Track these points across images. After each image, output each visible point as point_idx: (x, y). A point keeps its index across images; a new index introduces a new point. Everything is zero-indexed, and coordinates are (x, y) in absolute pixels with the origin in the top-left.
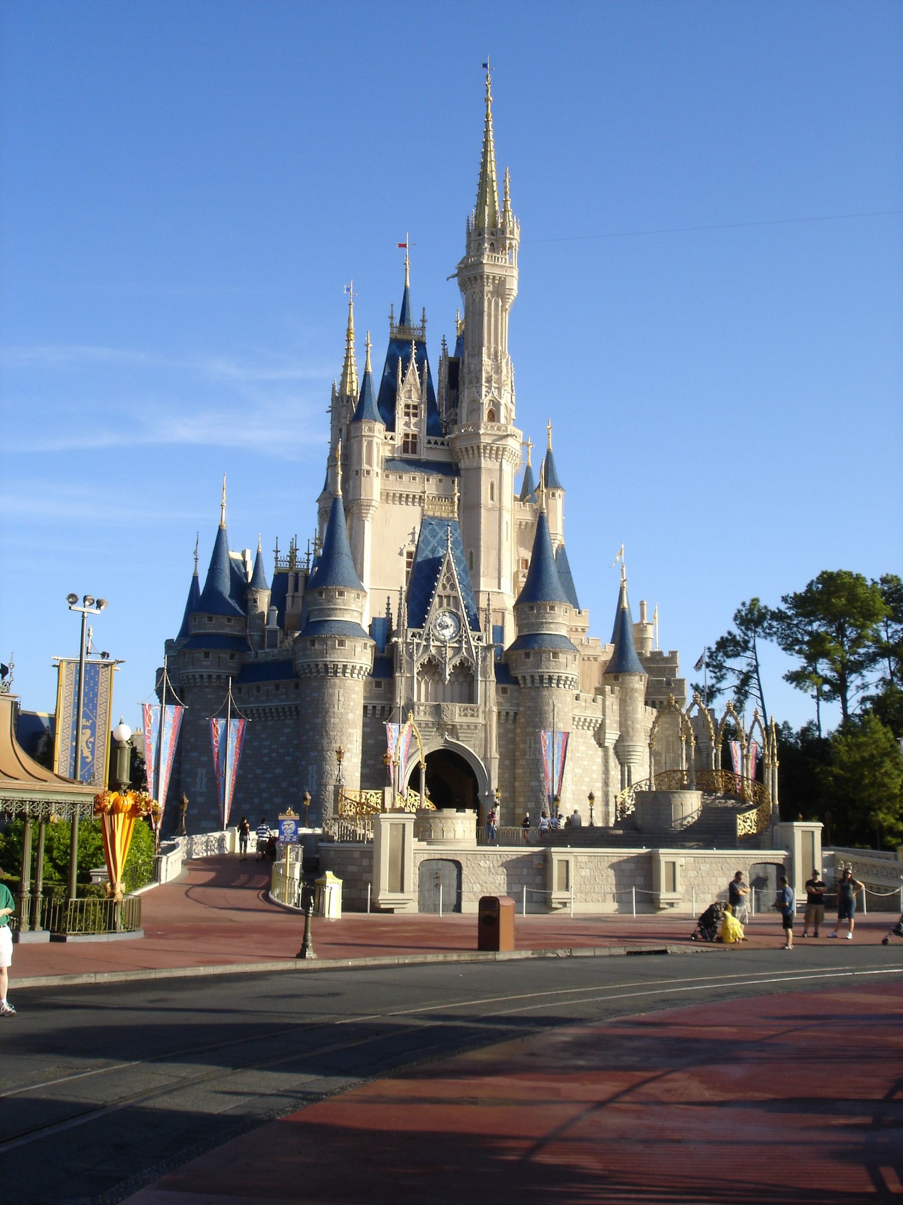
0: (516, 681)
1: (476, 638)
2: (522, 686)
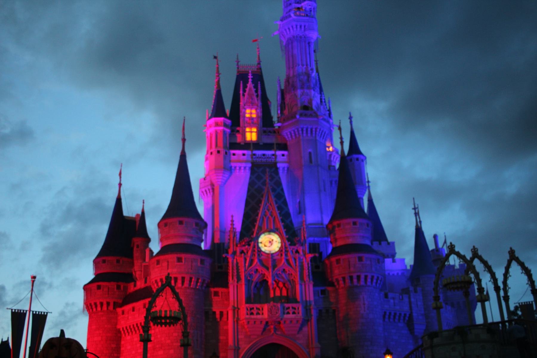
0: (332, 284)
1: (294, 251)
2: (337, 287)
